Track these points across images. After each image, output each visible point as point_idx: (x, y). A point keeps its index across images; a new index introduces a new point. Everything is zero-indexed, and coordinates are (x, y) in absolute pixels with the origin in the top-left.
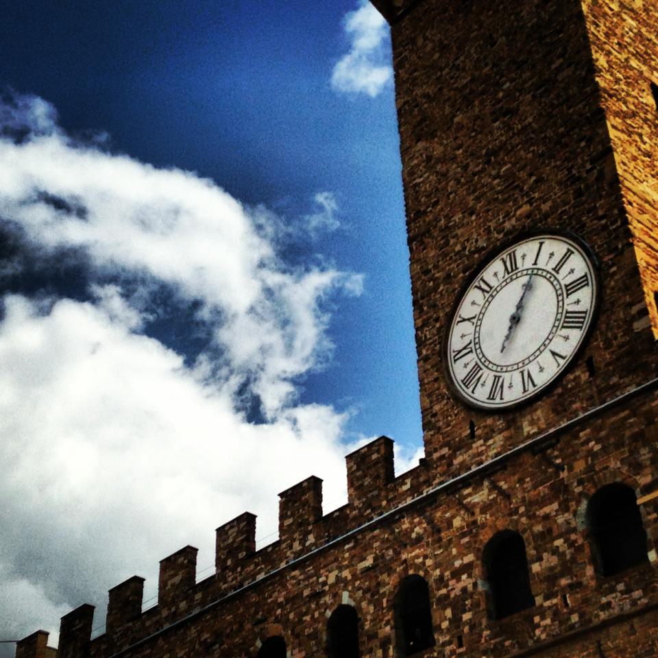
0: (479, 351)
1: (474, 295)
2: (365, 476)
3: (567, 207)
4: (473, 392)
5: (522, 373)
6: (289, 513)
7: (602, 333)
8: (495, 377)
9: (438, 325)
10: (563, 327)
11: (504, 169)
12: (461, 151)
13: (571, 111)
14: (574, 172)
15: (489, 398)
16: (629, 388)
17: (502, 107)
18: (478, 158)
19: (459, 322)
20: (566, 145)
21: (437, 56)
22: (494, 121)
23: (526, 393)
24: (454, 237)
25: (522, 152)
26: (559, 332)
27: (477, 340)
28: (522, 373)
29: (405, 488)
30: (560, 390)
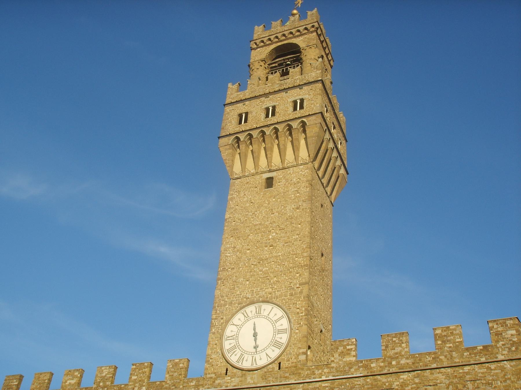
2: (175, 372)
5: (253, 357)
6: (136, 374)
7: (287, 355)
9: (222, 321)
12: (248, 251)
21: (248, 205)
22: (266, 246)
24: (237, 287)
28: (253, 357)
29: (192, 384)
30: (265, 370)
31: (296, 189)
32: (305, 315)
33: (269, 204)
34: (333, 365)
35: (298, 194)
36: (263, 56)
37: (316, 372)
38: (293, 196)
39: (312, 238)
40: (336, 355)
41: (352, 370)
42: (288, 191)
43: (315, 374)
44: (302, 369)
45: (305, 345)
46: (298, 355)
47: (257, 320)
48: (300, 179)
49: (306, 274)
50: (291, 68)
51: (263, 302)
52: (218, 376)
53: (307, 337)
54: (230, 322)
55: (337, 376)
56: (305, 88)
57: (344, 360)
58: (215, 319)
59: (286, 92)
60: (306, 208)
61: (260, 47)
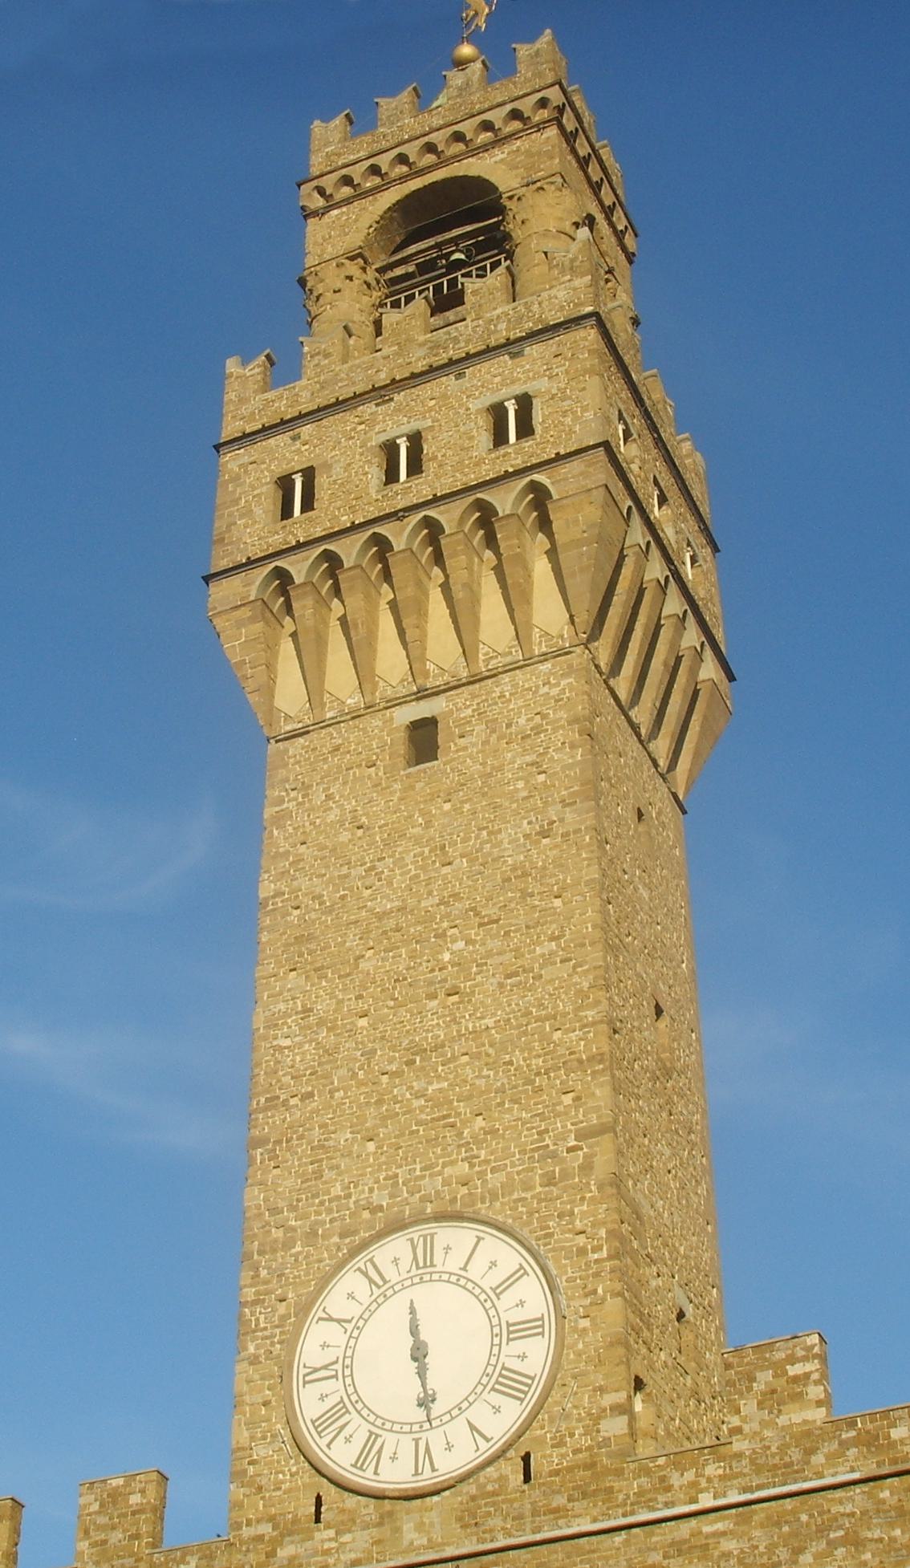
0: (348, 1381)
1: (350, 1281)
2: (113, 1528)
3: (528, 1195)
4: (328, 1446)
5: (417, 1441)
7: (552, 1421)
8: (371, 1433)
9: (282, 1309)
10: (493, 1389)
11: (435, 1086)
12: (363, 1022)
13: (557, 1035)
14: (548, 1141)
15: (354, 1466)
16: (578, 1520)
17: (445, 980)
18: (393, 1048)
19: (320, 1319)
20: (539, 1090)
21: (345, 837)
23: (419, 1478)
24: (331, 1168)
25: (468, 1070)
26: (485, 1395)
27: (348, 1362)
28: (417, 1441)
30: (470, 1488)
31: (534, 757)
32: (610, 1257)
33: (428, 824)
34: (739, 1445)
35: (541, 778)
36: (355, 239)
37: (676, 1480)
38: (521, 784)
39: (611, 948)
40: (749, 1406)
41: (818, 1459)
42: (500, 769)
43: (669, 1489)
44: (619, 1473)
45: (622, 1377)
46: (599, 1418)
47: (421, 1295)
48: (544, 717)
49: (601, 1093)
50: (468, 275)
51: (441, 1217)
52: (287, 1530)
53: (627, 1346)
54: (317, 1312)
55: (760, 1487)
56: (533, 351)
57: (782, 1421)
58: (255, 1303)
59: (460, 376)
60: (576, 832)
61: (337, 205)
